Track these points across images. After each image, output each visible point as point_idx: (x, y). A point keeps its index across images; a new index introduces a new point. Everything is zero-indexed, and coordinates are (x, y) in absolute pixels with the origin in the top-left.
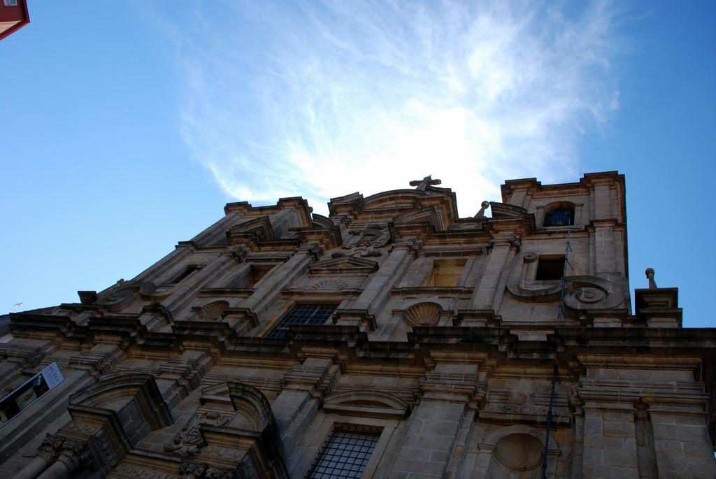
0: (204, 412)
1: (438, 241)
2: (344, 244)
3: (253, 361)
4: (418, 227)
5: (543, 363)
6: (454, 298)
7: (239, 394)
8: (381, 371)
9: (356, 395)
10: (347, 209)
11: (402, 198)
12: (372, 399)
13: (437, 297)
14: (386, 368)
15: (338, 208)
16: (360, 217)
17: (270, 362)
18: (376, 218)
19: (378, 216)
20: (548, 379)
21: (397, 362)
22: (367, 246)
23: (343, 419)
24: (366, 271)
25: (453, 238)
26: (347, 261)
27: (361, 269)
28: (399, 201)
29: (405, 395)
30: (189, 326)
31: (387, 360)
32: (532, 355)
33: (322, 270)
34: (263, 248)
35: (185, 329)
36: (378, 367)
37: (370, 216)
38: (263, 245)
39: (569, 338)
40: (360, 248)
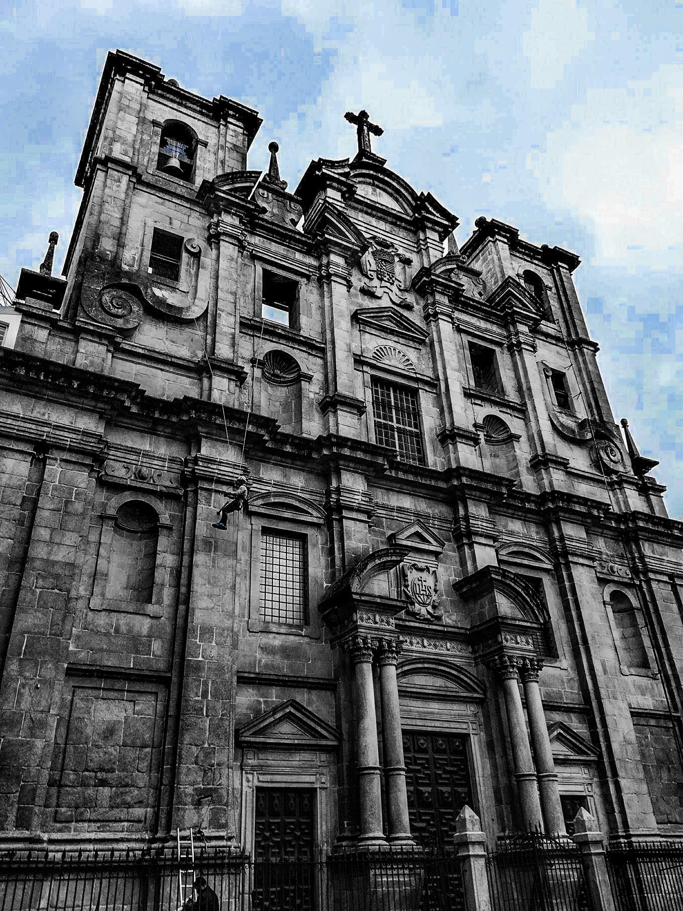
0: (413, 562)
8: (514, 514)
19: (370, 211)
26: (390, 313)
30: (349, 443)
34: (258, 231)
35: (346, 446)
39: (640, 519)
40: (384, 284)
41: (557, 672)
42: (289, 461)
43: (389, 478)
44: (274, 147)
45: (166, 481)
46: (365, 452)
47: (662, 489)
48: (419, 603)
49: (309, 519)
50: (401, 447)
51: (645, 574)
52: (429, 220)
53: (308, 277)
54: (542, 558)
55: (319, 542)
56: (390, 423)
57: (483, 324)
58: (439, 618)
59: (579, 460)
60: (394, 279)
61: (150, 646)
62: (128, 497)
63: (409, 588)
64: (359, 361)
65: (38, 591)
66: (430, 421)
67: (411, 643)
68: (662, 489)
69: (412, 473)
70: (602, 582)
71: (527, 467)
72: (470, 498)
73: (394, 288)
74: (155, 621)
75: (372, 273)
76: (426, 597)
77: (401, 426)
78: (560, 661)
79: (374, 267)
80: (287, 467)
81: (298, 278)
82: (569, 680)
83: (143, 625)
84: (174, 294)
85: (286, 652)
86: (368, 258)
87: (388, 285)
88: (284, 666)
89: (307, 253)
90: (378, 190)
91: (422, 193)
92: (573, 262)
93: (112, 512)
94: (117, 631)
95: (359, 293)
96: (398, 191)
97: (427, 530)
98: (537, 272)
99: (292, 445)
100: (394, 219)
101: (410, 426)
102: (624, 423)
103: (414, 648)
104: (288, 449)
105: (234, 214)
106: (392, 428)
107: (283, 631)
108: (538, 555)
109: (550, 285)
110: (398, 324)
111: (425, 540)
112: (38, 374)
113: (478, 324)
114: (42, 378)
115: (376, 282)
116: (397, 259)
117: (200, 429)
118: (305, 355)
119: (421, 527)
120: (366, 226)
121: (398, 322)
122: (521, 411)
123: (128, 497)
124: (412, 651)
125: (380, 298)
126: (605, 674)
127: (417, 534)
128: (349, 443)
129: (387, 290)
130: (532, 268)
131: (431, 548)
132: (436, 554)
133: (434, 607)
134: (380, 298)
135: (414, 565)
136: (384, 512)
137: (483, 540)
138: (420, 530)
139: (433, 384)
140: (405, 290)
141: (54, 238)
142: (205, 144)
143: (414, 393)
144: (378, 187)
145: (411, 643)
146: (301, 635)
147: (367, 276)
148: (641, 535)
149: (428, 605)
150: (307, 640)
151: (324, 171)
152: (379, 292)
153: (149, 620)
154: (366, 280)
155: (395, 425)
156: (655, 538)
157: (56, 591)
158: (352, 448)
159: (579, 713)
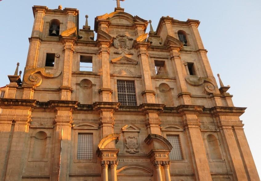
0: (129, 136)
2: (115, 46)
4: (146, 44)
7: (154, 137)
9: (168, 125)
12: (173, 126)
16: (110, 26)
18: (117, 28)
19: (117, 27)
23: (168, 133)
27: (132, 64)
28: (120, 17)
35: (102, 104)
38: (79, 43)
40: (122, 49)
41: (184, 164)
42: (86, 112)
43: (120, 111)
44: (87, 17)
45: (50, 125)
46: (109, 105)
47: (231, 96)
49: (93, 128)
50: (128, 100)
51: (221, 127)
52: (137, 24)
53: (95, 54)
55: (97, 134)
56: (124, 93)
57: (161, 53)
58: (138, 152)
59: (196, 91)
60: (126, 47)
61: (45, 169)
62: (38, 130)
63: (127, 144)
64: (112, 76)
65: (13, 158)
66: (138, 90)
67: (128, 161)
68: (231, 96)
69: (128, 108)
70: (203, 132)
71: (177, 98)
73: (126, 49)
74: (46, 163)
75: (118, 47)
76: (133, 146)
77: (129, 93)
78: (185, 160)
79: (119, 44)
80: (86, 114)
81: (91, 55)
83: (43, 164)
84: (52, 71)
85: (86, 167)
86: (116, 42)
87: (124, 49)
88: (85, 172)
89: (96, 46)
90: (121, 19)
91: (135, 16)
92: (197, 22)
93: (34, 135)
94: (36, 166)
96: (128, 18)
97: (134, 125)
98: (183, 30)
99: (86, 107)
100: (127, 27)
101: (132, 92)
102: (218, 75)
103: (129, 162)
104: (85, 108)
105: (70, 42)
106: (125, 95)
107: (85, 161)
108: (177, 127)
109: (189, 33)
110: (127, 61)
111: (135, 129)
112: (10, 103)
113: (159, 54)
114: (11, 103)
115: (120, 49)
116: (127, 40)
117: (56, 108)
118: (94, 78)
119: (132, 125)
120: (116, 32)
121: (127, 60)
122: (175, 79)
123: (38, 130)
124: (128, 163)
125: (121, 54)
126: (200, 162)
127: (131, 127)
128: (103, 103)
129: (123, 51)
130: (181, 29)
131: (135, 131)
132: (138, 132)
133: (136, 149)
134: (121, 54)
135: (129, 137)
137: (154, 125)
138: (132, 126)
139: (140, 77)
140: (131, 49)
141: (18, 64)
142: (62, 23)
143: (133, 82)
144: (121, 18)
145: (128, 161)
146: (90, 162)
147: (116, 48)
148: (220, 114)
149: (134, 148)
150: (92, 163)
152: (120, 52)
153: (44, 163)
154: (116, 49)
155: (126, 93)
156: (225, 113)
157: (18, 158)
158: (104, 105)
159: (191, 176)
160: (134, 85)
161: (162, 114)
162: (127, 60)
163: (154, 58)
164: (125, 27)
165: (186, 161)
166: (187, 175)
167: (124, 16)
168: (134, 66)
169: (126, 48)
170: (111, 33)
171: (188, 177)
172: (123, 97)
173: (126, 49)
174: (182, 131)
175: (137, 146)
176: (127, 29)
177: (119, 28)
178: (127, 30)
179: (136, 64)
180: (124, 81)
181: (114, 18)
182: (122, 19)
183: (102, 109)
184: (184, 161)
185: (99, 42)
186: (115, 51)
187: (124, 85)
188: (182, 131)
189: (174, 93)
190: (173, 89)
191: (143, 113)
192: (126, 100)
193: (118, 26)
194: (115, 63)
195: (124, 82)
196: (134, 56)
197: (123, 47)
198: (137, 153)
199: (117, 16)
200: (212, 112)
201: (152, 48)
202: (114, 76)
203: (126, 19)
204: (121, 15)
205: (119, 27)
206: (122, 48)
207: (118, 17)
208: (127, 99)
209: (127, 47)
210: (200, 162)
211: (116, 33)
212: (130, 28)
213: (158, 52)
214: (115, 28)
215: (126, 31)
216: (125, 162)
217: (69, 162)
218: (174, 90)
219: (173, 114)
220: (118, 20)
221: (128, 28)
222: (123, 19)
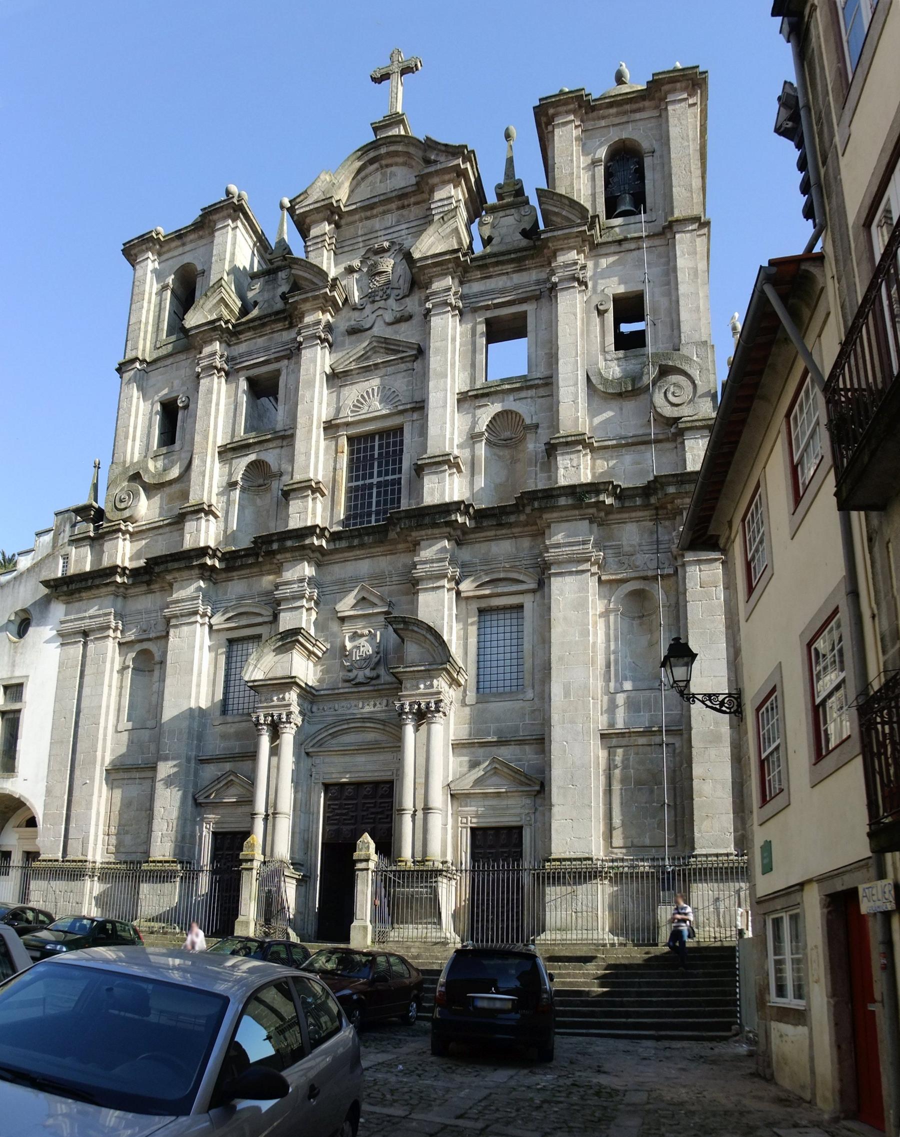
1: (478, 274)
3: (358, 553)
5: (646, 506)
6: (531, 398)
9: (486, 574)
10: (321, 215)
11: (389, 154)
12: (502, 575)
13: (511, 398)
14: (499, 532)
15: (306, 217)
17: (378, 549)
18: (367, 218)
19: (369, 213)
20: (651, 520)
21: (510, 525)
22: (385, 300)
23: (484, 604)
24: (408, 359)
25: (497, 266)
27: (402, 358)
28: (384, 162)
29: (528, 562)
31: (500, 525)
32: (636, 501)
33: (351, 370)
36: (492, 533)
37: (357, 217)
40: (377, 305)
41: (518, 705)
48: (356, 668)
54: (521, 578)
58: (378, 677)
72: (423, 540)
73: (391, 302)
82: (533, 711)
90: (389, 170)
95: (347, 337)
115: (369, 308)
121: (385, 348)
126: (565, 697)
127: (364, 598)
129: (380, 312)
133: (373, 669)
136: (337, 587)
144: (387, 166)
149: (366, 668)
151: (297, 212)
154: (356, 314)
160: (402, 442)
161: (472, 536)
162: (385, 348)
163: (487, 308)
164: (393, 206)
165: (530, 694)
166: (521, 742)
167: (396, 154)
168: (409, 365)
169: (389, 297)
170: (346, 249)
171: (527, 747)
172: (363, 496)
173: (391, 302)
174: (534, 591)
175: (375, 660)
176: (403, 207)
177: (376, 216)
178: (405, 212)
179: (415, 358)
180: (370, 436)
181: (363, 174)
182: (394, 169)
183: (278, 557)
184: (521, 696)
185: (296, 308)
186: (353, 323)
187: (373, 448)
188: (534, 591)
189: (534, 446)
190: (537, 426)
191: (407, 545)
192: (370, 504)
193: (371, 207)
194: (346, 373)
195: (373, 440)
196: (414, 321)
197: (377, 298)
198: (374, 682)
199: (371, 161)
200: (653, 500)
201: (480, 267)
202: (337, 426)
203: (405, 164)
204: (383, 150)
205: (375, 212)
206: (374, 302)
207: (376, 166)
208: (374, 500)
209: (396, 292)
210: (567, 694)
211: (361, 245)
212: (412, 200)
213: (504, 278)
214: (361, 220)
215: (398, 223)
216: (338, 712)
217: (196, 725)
218: (539, 431)
219: (509, 531)
220: (378, 175)
221: (406, 203)
222: (397, 164)
